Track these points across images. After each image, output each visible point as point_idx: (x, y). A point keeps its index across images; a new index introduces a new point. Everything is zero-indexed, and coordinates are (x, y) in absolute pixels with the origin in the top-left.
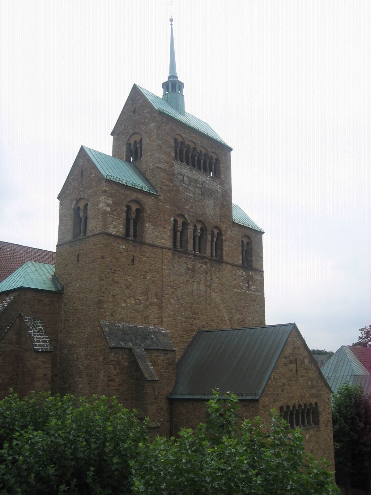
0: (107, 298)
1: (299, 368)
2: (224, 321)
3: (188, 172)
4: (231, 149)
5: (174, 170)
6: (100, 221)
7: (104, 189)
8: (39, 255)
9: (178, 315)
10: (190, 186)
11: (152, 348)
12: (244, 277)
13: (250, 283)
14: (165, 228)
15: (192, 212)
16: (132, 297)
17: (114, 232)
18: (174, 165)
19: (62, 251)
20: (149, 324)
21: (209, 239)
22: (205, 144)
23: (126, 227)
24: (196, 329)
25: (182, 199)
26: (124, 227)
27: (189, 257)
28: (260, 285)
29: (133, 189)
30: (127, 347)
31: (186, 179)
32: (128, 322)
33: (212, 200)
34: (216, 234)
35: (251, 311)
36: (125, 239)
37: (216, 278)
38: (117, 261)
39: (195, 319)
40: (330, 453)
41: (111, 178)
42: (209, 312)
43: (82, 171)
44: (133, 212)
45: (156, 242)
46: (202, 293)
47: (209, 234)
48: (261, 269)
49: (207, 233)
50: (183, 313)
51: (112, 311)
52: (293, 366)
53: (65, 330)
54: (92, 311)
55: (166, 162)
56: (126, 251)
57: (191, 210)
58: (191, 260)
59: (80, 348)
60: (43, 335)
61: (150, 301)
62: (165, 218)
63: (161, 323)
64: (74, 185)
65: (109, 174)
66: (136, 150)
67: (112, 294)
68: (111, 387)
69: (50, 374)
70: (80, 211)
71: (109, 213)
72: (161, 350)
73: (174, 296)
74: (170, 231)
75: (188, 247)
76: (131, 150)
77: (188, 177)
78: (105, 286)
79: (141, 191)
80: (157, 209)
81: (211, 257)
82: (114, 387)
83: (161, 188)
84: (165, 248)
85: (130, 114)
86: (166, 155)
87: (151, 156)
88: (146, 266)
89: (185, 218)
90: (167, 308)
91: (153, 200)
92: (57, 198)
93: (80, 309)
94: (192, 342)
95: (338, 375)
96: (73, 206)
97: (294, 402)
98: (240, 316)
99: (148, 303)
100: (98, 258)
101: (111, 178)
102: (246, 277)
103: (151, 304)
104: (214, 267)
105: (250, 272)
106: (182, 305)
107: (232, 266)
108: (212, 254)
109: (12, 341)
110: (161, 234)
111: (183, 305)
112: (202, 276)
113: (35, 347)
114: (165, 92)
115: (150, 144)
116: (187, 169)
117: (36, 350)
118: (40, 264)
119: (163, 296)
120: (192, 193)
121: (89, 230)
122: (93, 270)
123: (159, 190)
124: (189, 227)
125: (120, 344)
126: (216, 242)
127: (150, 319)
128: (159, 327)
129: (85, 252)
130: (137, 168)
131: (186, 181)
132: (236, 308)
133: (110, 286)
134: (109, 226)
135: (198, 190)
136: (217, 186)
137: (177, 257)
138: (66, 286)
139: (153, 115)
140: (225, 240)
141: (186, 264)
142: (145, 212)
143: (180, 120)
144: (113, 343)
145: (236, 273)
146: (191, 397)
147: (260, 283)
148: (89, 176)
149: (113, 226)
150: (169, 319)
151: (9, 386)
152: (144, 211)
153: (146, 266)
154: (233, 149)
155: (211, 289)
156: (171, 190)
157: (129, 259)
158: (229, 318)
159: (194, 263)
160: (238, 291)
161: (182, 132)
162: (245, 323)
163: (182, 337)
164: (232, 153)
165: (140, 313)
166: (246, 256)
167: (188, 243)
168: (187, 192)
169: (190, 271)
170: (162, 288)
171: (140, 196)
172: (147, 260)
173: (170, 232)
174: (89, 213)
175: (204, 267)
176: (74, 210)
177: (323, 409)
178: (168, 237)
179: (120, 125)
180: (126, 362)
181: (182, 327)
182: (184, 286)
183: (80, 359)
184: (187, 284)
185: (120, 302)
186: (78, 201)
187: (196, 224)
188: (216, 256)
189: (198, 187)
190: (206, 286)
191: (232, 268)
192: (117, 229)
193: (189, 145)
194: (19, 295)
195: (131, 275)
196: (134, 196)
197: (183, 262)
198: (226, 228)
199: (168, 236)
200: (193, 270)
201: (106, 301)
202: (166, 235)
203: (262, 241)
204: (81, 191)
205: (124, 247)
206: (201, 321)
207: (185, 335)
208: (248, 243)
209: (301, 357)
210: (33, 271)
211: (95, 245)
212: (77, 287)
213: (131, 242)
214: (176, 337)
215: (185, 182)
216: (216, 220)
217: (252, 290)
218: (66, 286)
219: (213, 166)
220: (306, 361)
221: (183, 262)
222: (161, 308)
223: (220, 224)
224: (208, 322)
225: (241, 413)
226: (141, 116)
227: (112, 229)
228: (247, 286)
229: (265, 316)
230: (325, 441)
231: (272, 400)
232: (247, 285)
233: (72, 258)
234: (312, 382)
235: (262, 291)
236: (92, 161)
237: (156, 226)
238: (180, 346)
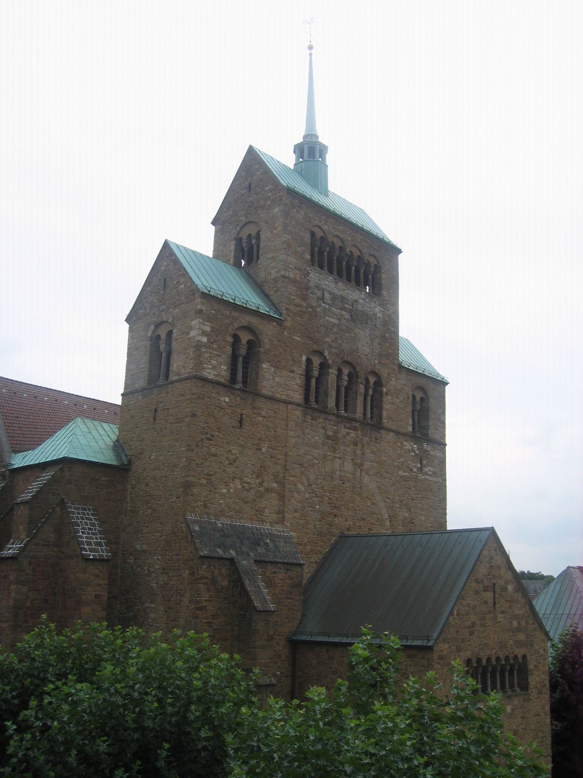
0: (199, 479)
1: (498, 598)
2: (382, 520)
3: (330, 284)
4: (399, 251)
6: (191, 359)
7: (198, 307)
8: (95, 409)
9: (309, 509)
10: (333, 307)
11: (266, 559)
13: (424, 462)
14: (292, 372)
15: (336, 347)
16: (238, 479)
17: (214, 377)
19: (131, 402)
20: (263, 521)
21: (361, 391)
22: (358, 241)
23: (232, 369)
24: (337, 532)
25: (321, 326)
26: (228, 369)
27: (329, 418)
28: (439, 465)
29: (244, 310)
30: (228, 557)
31: (327, 296)
32: (231, 517)
33: (367, 330)
34: (372, 384)
35: (425, 506)
36: (229, 387)
37: (371, 453)
38: (216, 421)
39: (335, 515)
40: (545, 737)
41: (210, 291)
42: (359, 507)
43: (165, 280)
44: (243, 345)
45: (278, 393)
46: (349, 475)
47: (362, 384)
48: (442, 441)
49: (357, 382)
50: (317, 507)
51: (206, 499)
52: (489, 595)
53: (132, 527)
54: (174, 499)
55: (296, 268)
56: (231, 406)
57: (334, 345)
58: (332, 423)
59: (154, 556)
60: (96, 534)
61: (266, 486)
62: (292, 356)
63: (282, 521)
64: (152, 301)
65: (207, 285)
66: (251, 248)
67: (206, 473)
68: (201, 618)
69: (105, 596)
70: (161, 342)
71: (205, 345)
72: (280, 563)
73: (304, 479)
74: (301, 376)
75: (327, 404)
76: (243, 249)
77: (330, 293)
78: (196, 460)
79: (256, 313)
80: (280, 341)
81: (364, 419)
82: (203, 619)
83: (287, 309)
84: (291, 403)
85: (243, 192)
86: (297, 257)
87: (273, 258)
88: (262, 430)
89: (325, 357)
90: (292, 497)
91: (274, 326)
92: (126, 321)
93: (156, 496)
94: (331, 551)
95: (560, 612)
96: (149, 334)
97: (488, 652)
98: (407, 515)
99: (262, 489)
100: (187, 416)
101: (210, 291)
102: (417, 452)
103: (268, 490)
104: (368, 436)
105: (425, 445)
106: (316, 494)
107: (396, 435)
108: (365, 414)
109: (49, 542)
110: (285, 382)
111: (318, 493)
112: (349, 449)
113: (83, 552)
114: (297, 159)
115: (272, 240)
117: (85, 557)
118: (96, 423)
119: (286, 478)
121: (173, 372)
122: (177, 434)
123: (284, 312)
124: (330, 371)
125: (217, 551)
126: (372, 397)
127: (264, 514)
128: (279, 528)
129: (166, 406)
130: (251, 277)
131: (328, 299)
132: (401, 501)
133: (204, 460)
134: (205, 365)
135: (345, 313)
136: (376, 307)
137: (310, 418)
138: (136, 457)
139: (279, 194)
140: (387, 394)
141: (324, 429)
142: (262, 346)
143: (320, 202)
144: (206, 551)
145: (402, 446)
146: (326, 639)
147: (440, 462)
148: (176, 288)
149: (210, 367)
150: (297, 514)
151: (41, 612)
152: (260, 345)
153: (262, 430)
154: (402, 250)
155: (361, 470)
156: (304, 312)
157: (235, 418)
158: (389, 516)
160: (405, 474)
161: (323, 221)
162: (415, 526)
163: (314, 544)
164: (401, 257)
165: (250, 504)
166: (418, 419)
167: (328, 396)
168: (329, 316)
169: (330, 441)
170: (285, 466)
171: (254, 321)
172: (263, 420)
173: (300, 378)
174: (174, 345)
175: (352, 435)
176: (150, 340)
177: (535, 666)
178: (297, 387)
179: (227, 209)
180: (224, 580)
181: (315, 528)
183: (153, 574)
184: (324, 461)
185: (219, 485)
186: (158, 326)
187: (341, 367)
188: (371, 418)
189: (346, 308)
190: (355, 464)
191: (397, 437)
192: (218, 372)
193: (332, 242)
194: (61, 470)
195: (237, 444)
196: (246, 320)
197: (320, 426)
198: (389, 374)
199: (297, 384)
200: (334, 439)
201: (196, 484)
202: (293, 383)
203: (444, 397)
204: (163, 311)
205: (227, 400)
206: (344, 519)
207: (320, 540)
208: (422, 399)
209: (502, 583)
210: (84, 433)
211: (183, 395)
212: (152, 460)
213: (239, 392)
214: (305, 544)
215: (325, 301)
216: (373, 362)
217: (426, 473)
218: (136, 457)
219: (371, 276)
220: (510, 588)
221: (320, 426)
222: (282, 497)
223: (379, 368)
224: (356, 521)
225: (404, 667)
226: (260, 196)
228: (420, 466)
229: (446, 515)
230: (536, 717)
231: (454, 648)
232: (419, 465)
233: (146, 415)
234: (519, 622)
235: (442, 475)
236: (181, 264)
237: (278, 368)
238: (310, 558)
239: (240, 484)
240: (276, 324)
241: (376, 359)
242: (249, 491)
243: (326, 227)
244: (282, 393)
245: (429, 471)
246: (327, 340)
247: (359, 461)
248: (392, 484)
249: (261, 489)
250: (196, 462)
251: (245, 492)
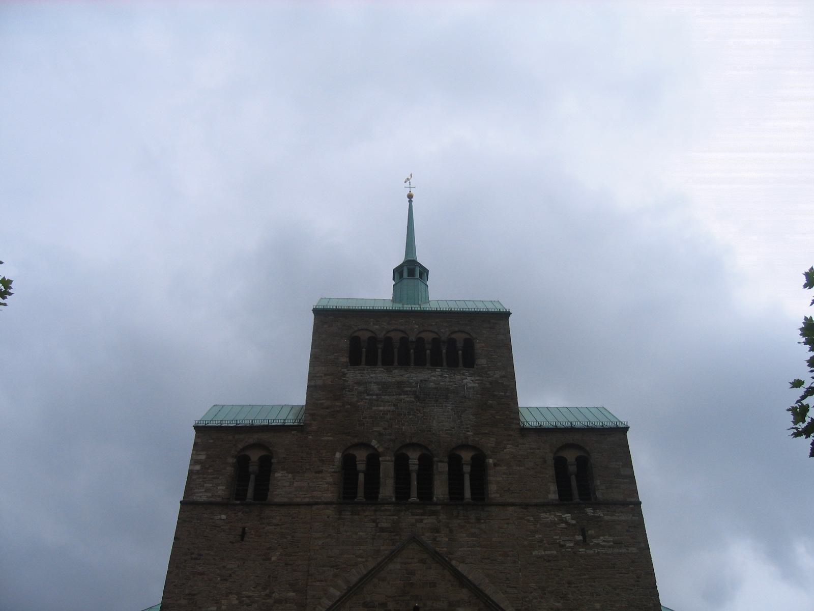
4: (508, 314)
5: (345, 381)
10: (385, 395)
12: (566, 523)
18: (344, 374)
22: (432, 325)
25: (365, 418)
27: (383, 508)
28: (627, 531)
31: (375, 387)
48: (628, 500)
55: (325, 375)
67: (187, 592)
71: (198, 472)
74: (332, 474)
84: (316, 504)
89: (373, 447)
99: (270, 601)
103: (279, 601)
110: (308, 484)
116: (377, 372)
120: (389, 406)
124: (381, 459)
135: (405, 396)
159: (396, 517)
160: (547, 552)
164: (511, 319)
168: (377, 406)
172: (275, 529)
173: (331, 476)
175: (425, 521)
178: (327, 486)
182: (367, 561)
189: (407, 391)
191: (525, 510)
196: (254, 438)
199: (327, 483)
202: (321, 483)
205: (224, 517)
217: (598, 545)
227: (201, 494)
232: (579, 538)
239: (237, 599)
240: (295, 432)
241: (468, 431)
242: (251, 605)
243: (377, 327)
244: (303, 496)
245: (604, 541)
246: (375, 430)
247: (445, 549)
248: (520, 569)
249: (268, 600)
250: (174, 584)
251: (245, 606)
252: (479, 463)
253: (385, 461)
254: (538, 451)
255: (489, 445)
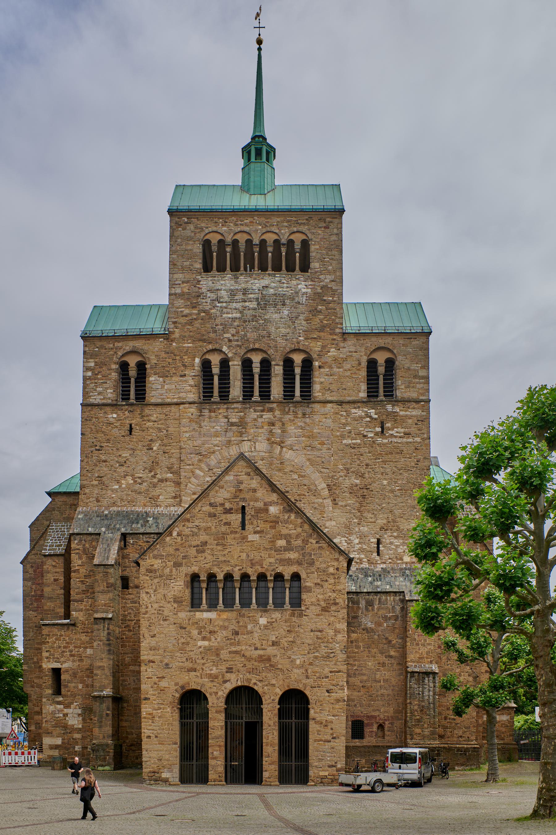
21: (276, 372)
26: (114, 391)
45: (168, 398)
71: (90, 378)
84: (183, 403)
124: (230, 363)
134: (91, 394)
178: (190, 388)
213: (127, 407)
227: (95, 397)
237: (167, 376)
252: (307, 364)
253: (234, 365)
254: (355, 354)
255: (316, 349)
